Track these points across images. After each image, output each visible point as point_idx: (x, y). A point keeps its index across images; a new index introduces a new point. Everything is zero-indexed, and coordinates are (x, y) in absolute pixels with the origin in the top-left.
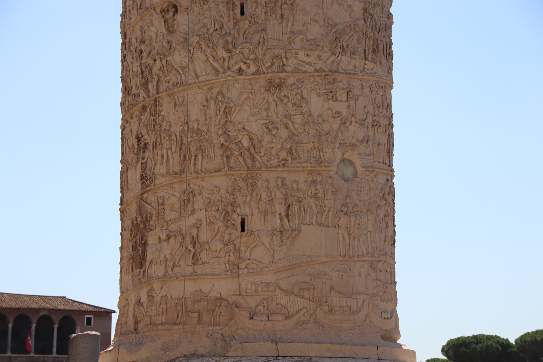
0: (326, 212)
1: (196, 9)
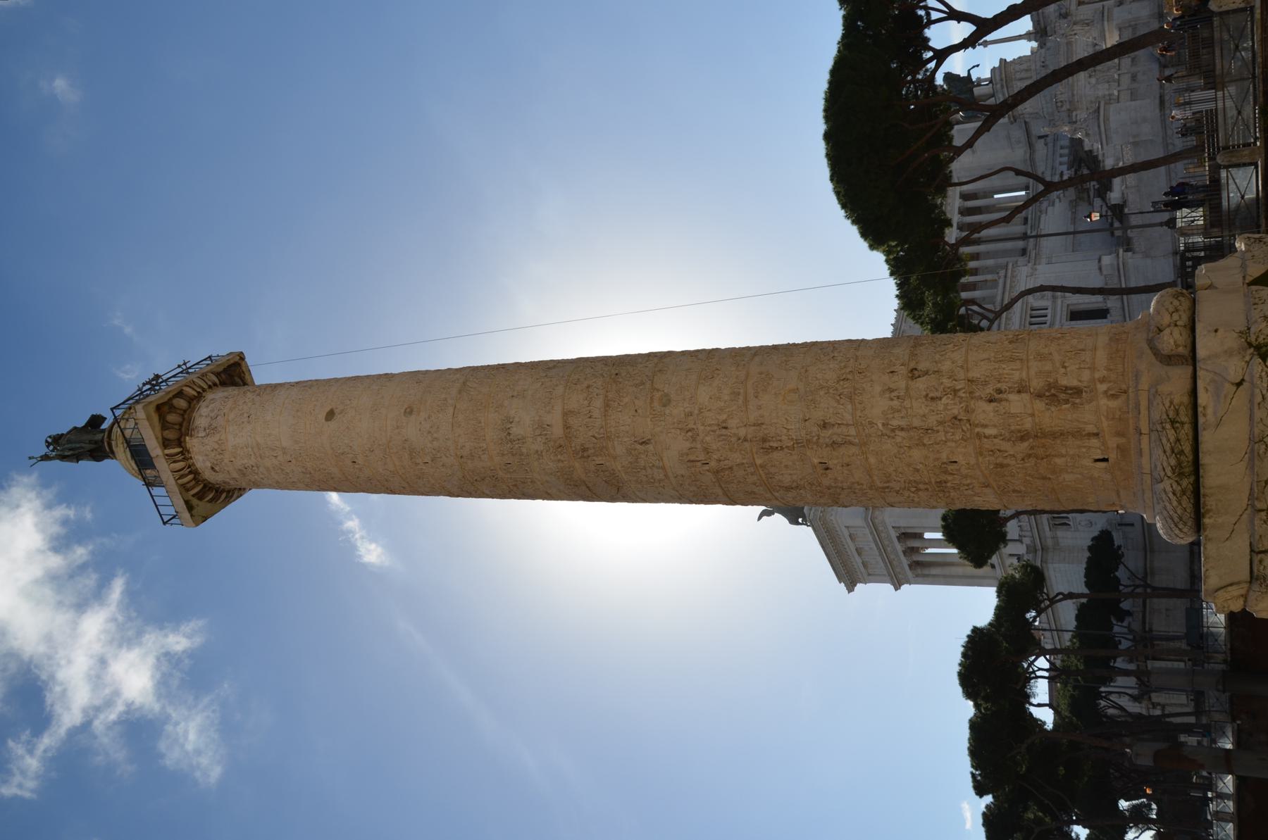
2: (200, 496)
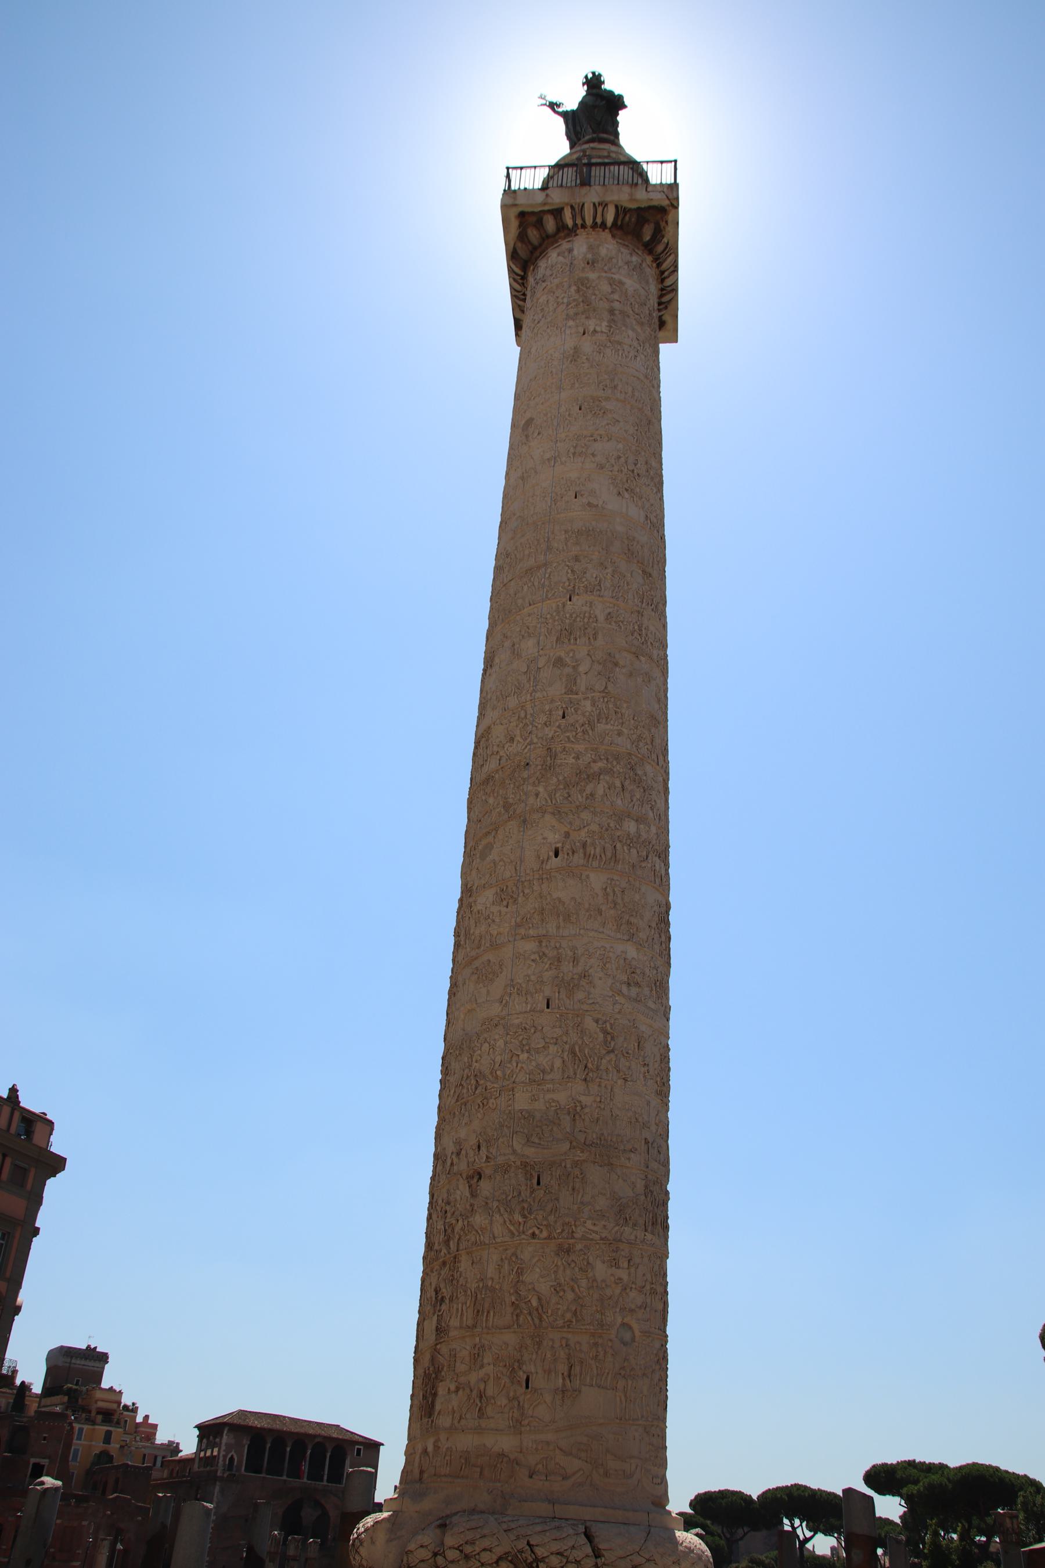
0: (606, 1374)
1: (498, 1178)
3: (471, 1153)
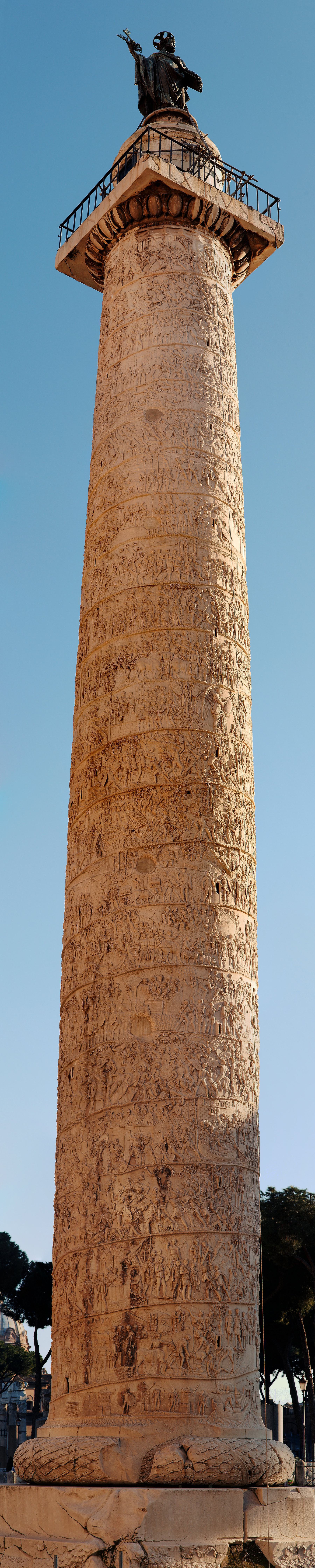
2: (89, 261)
3: (158, 1151)
